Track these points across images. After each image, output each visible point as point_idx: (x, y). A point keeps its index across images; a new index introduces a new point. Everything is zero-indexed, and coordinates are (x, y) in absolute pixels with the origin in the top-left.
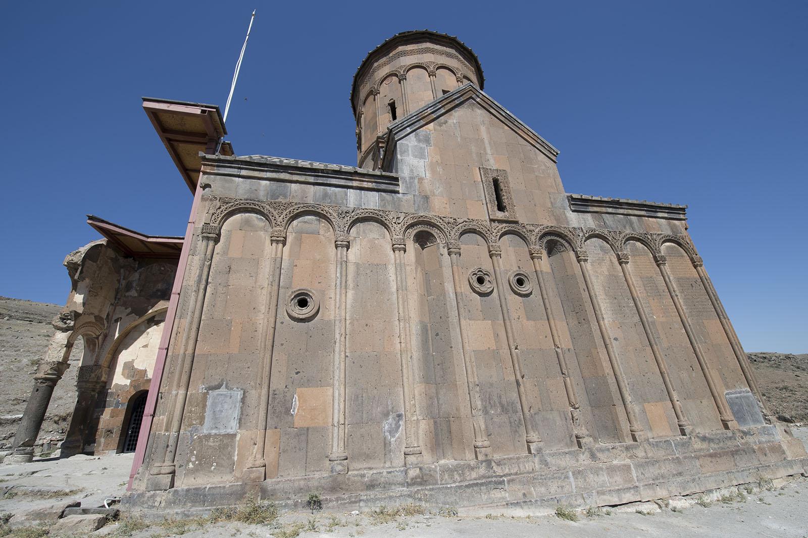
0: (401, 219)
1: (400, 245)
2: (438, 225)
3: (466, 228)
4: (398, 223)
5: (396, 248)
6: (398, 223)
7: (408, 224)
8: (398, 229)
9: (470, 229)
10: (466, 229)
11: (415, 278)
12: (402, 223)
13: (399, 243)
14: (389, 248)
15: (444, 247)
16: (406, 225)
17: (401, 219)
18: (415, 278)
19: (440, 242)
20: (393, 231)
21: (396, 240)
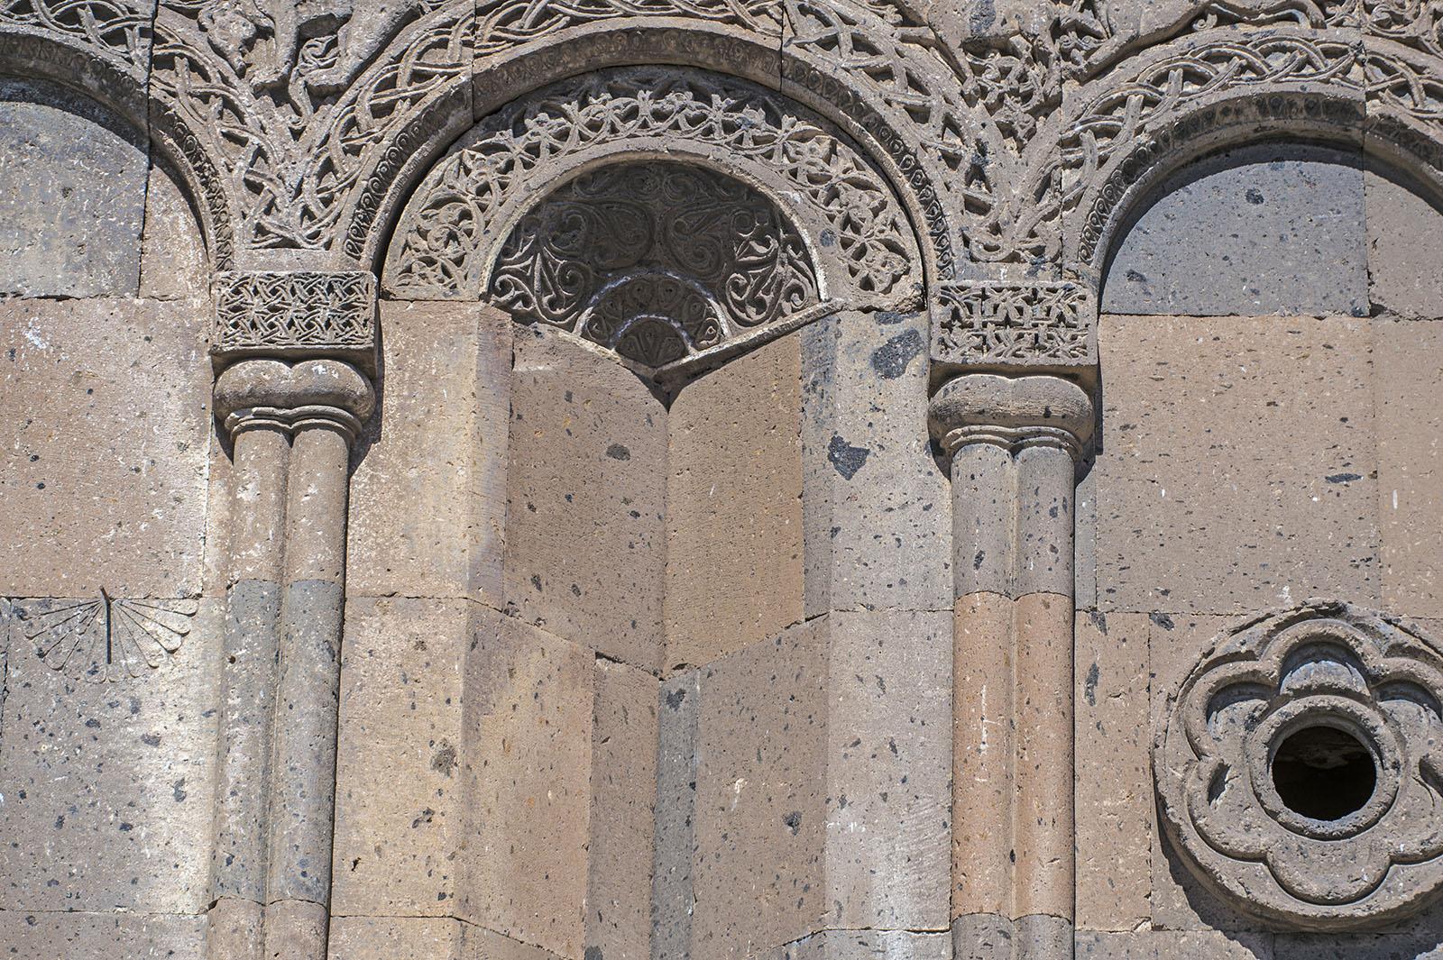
0: (357, 41)
1: (291, 359)
2: (832, 87)
3: (1209, 97)
4: (322, 96)
5: (242, 403)
6: (322, 96)
7: (436, 90)
8: (303, 167)
9: (1272, 104)
10: (1208, 117)
11: (444, 761)
12: (365, 94)
13: (288, 339)
14: (174, 406)
15: (886, 363)
16: (405, 115)
17: (357, 41)
18: (444, 761)
19: (849, 294)
20: (236, 197)
21: (256, 306)
